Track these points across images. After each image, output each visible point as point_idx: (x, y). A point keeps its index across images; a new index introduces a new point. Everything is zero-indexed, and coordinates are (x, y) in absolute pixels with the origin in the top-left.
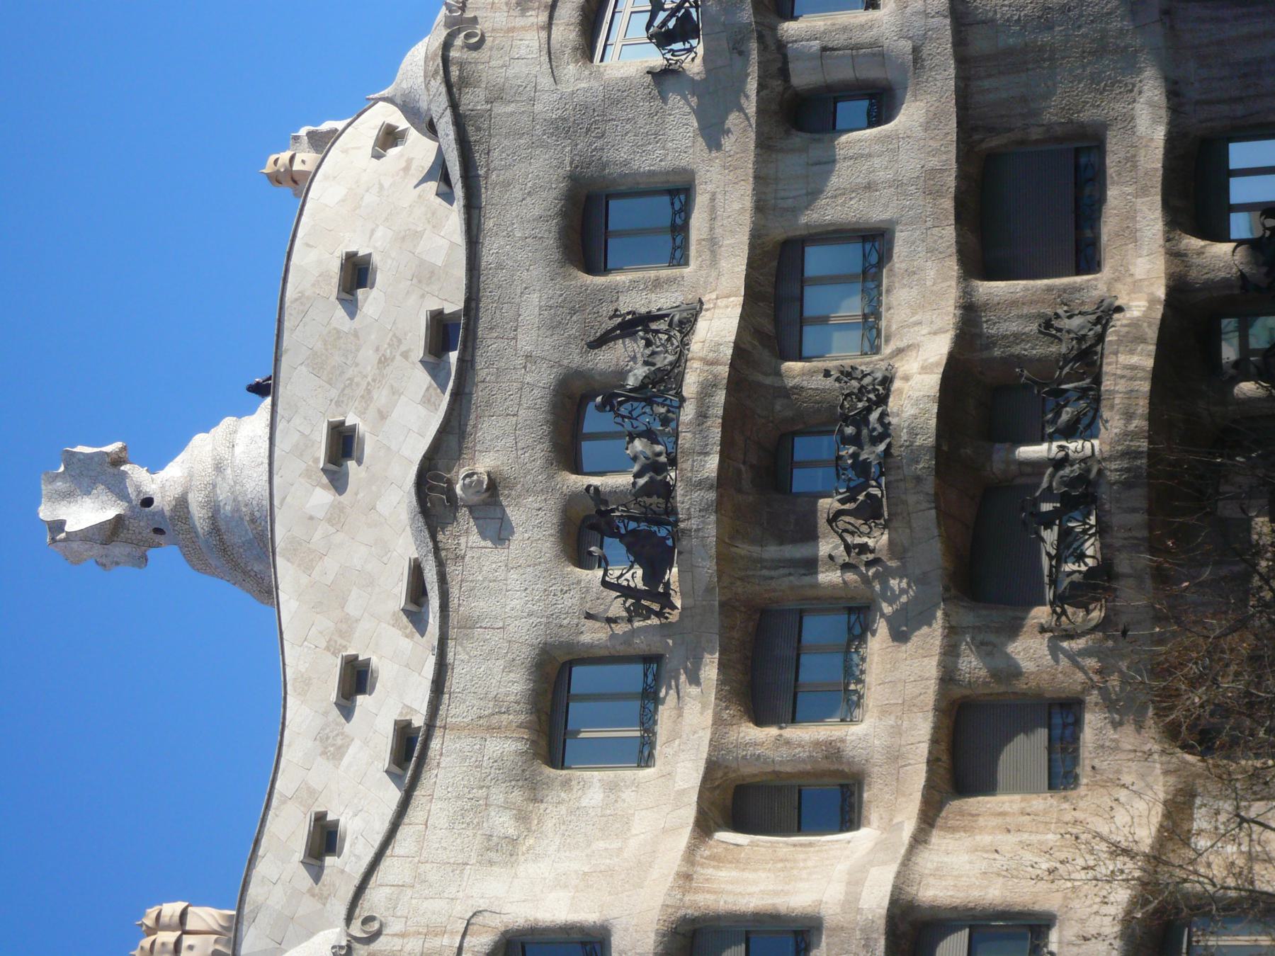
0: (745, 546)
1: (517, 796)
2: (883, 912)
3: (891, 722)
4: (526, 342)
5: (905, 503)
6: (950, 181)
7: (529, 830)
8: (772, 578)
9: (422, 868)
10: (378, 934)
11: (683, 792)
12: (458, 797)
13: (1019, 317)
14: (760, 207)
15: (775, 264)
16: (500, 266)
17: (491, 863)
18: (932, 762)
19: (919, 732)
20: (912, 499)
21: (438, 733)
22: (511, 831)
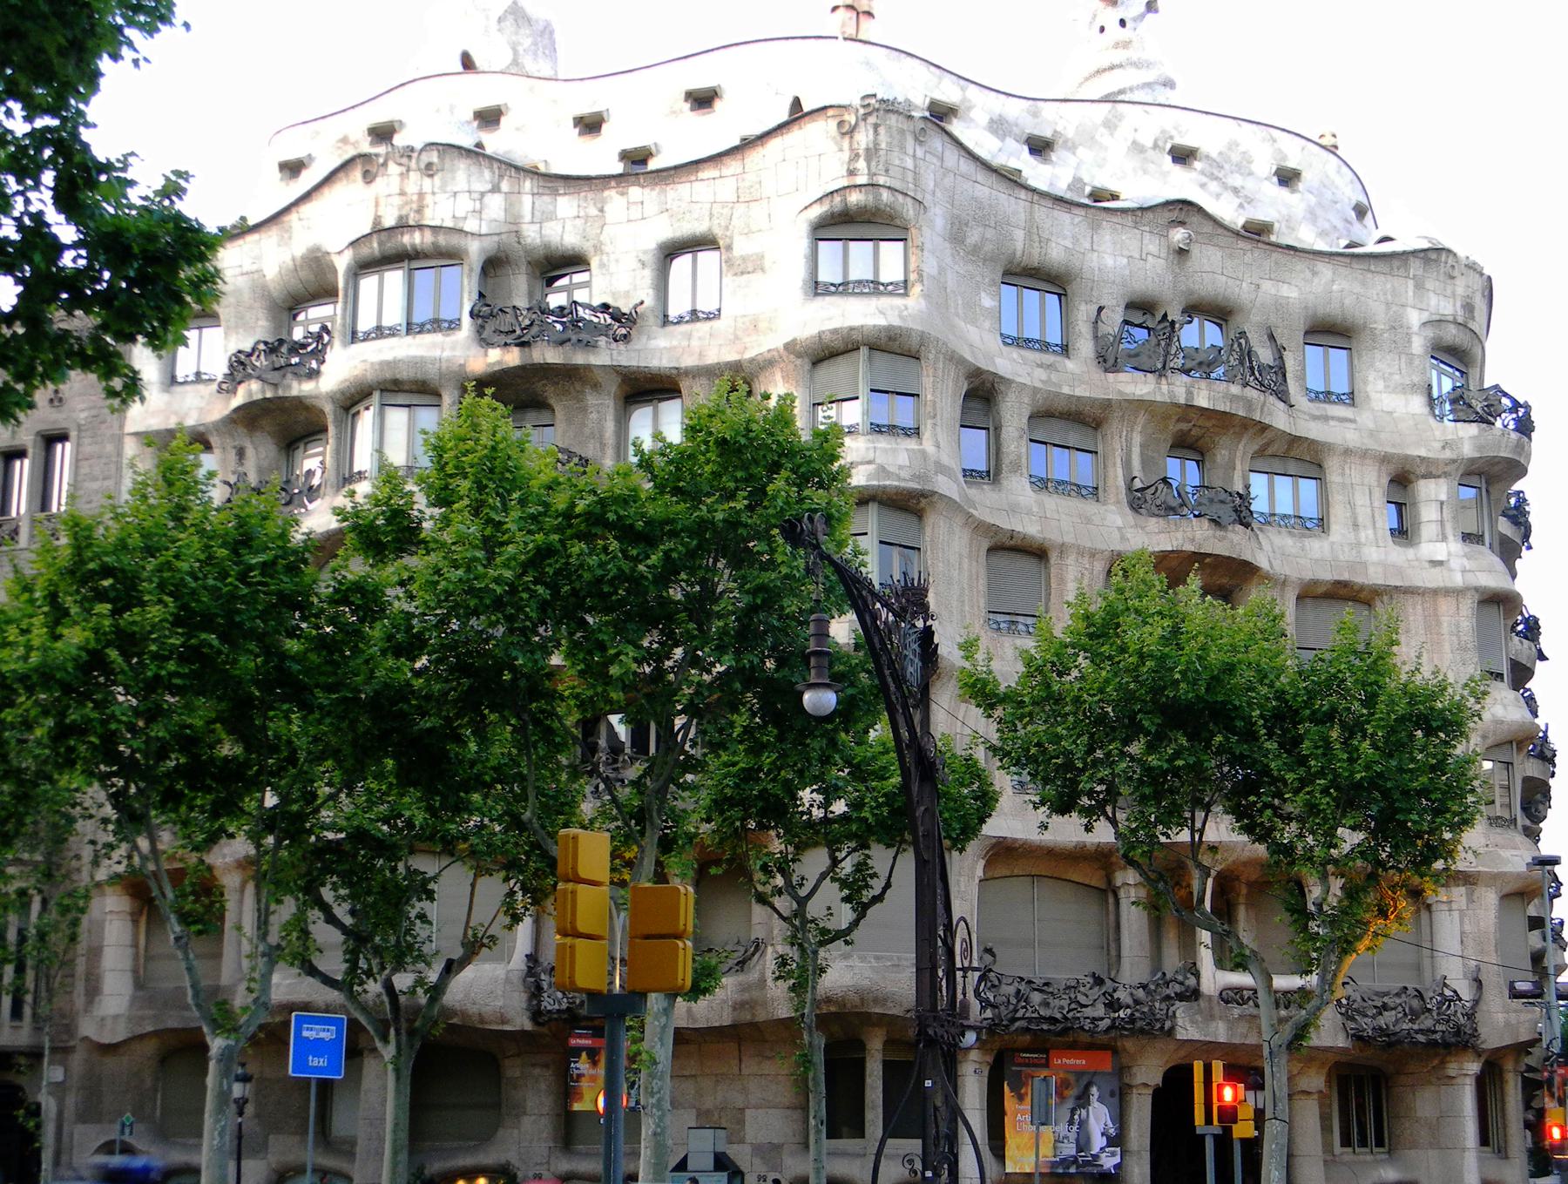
1: (988, 247)
4: (1267, 286)
6: (1359, 579)
10: (916, 139)
14: (1347, 452)
16: (1315, 274)
19: (1029, 528)
20: (1179, 535)
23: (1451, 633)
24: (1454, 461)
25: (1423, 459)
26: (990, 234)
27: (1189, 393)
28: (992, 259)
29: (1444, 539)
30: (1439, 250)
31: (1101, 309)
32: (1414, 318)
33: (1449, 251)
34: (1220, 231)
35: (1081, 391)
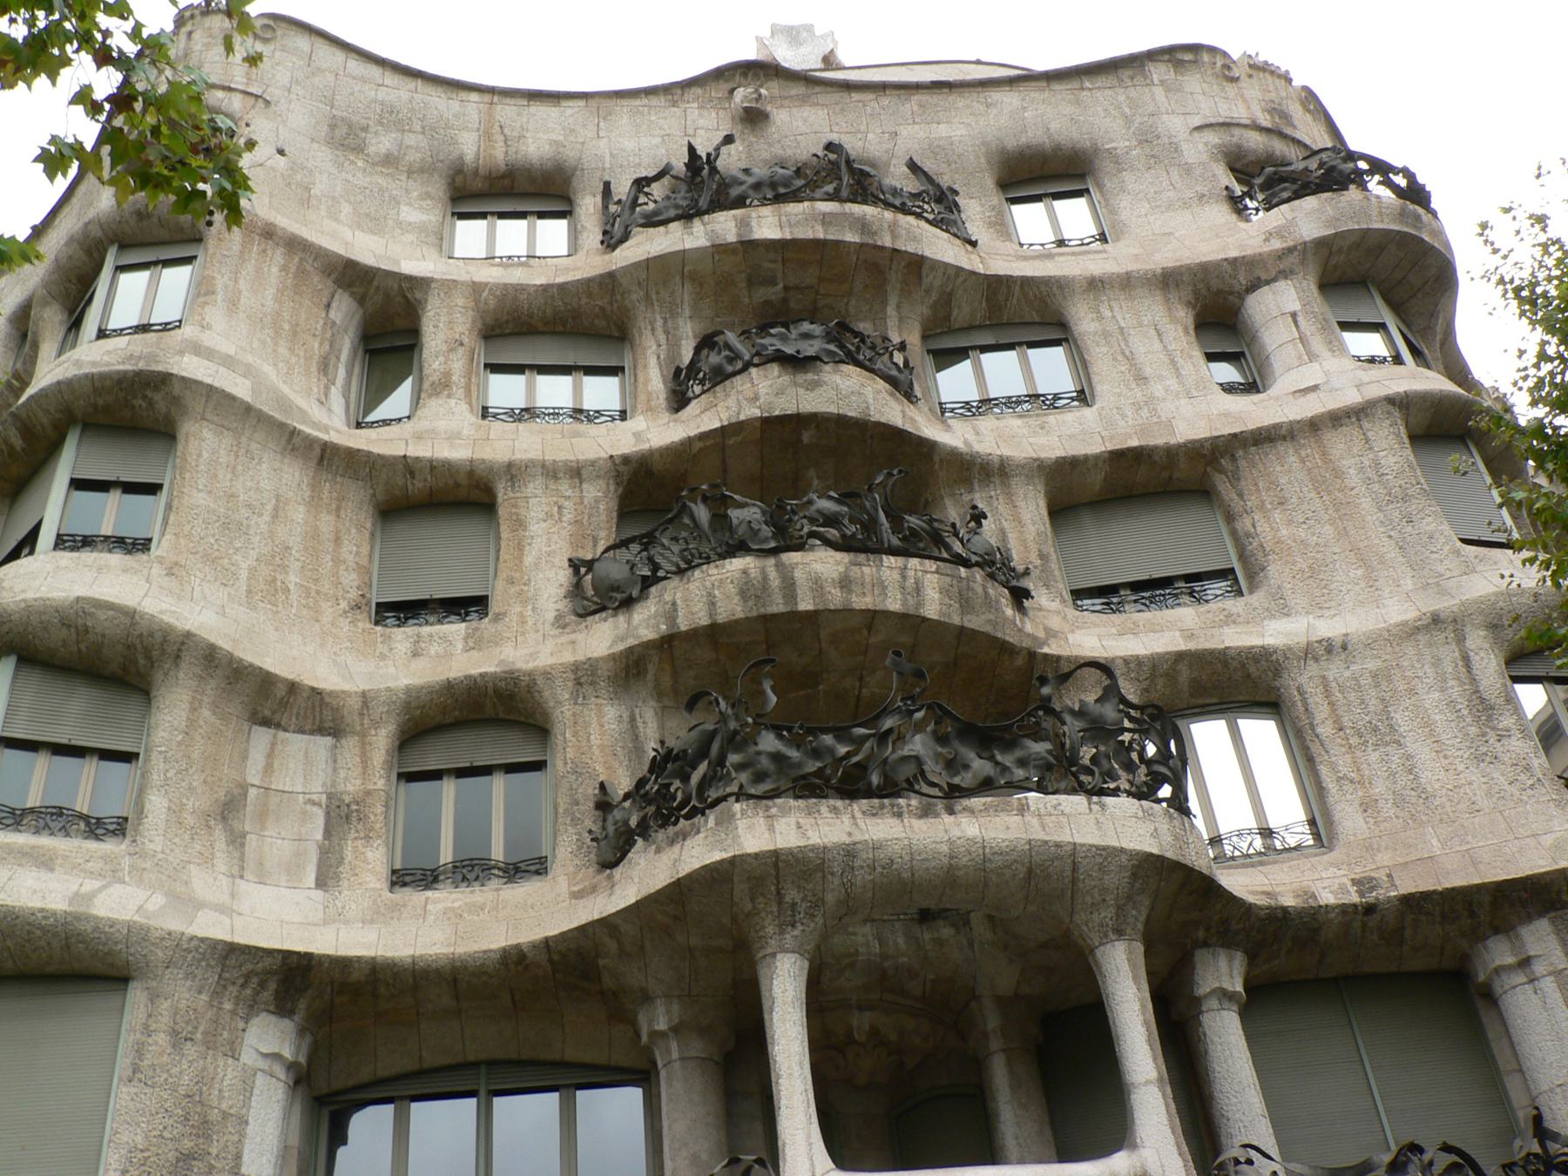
0: (686, 297)
1: (413, 157)
2: (174, 371)
3: (465, 432)
5: (727, 396)
6: (1158, 440)
7: (374, 164)
8: (653, 329)
9: (330, 77)
11: (397, 263)
12: (412, 110)
13: (1003, 532)
14: (1095, 285)
15: (1037, 319)
17: (333, 127)
18: (408, 466)
20: (731, 402)
21: (487, 98)
22: (371, 150)
23: (1368, 481)
24: (1290, 250)
25: (1234, 262)
26: (411, 140)
27: (744, 224)
28: (422, 171)
29: (1312, 357)
30: (1195, 48)
31: (607, 185)
32: (1175, 125)
33: (1212, 50)
34: (818, 89)
35: (559, 280)
